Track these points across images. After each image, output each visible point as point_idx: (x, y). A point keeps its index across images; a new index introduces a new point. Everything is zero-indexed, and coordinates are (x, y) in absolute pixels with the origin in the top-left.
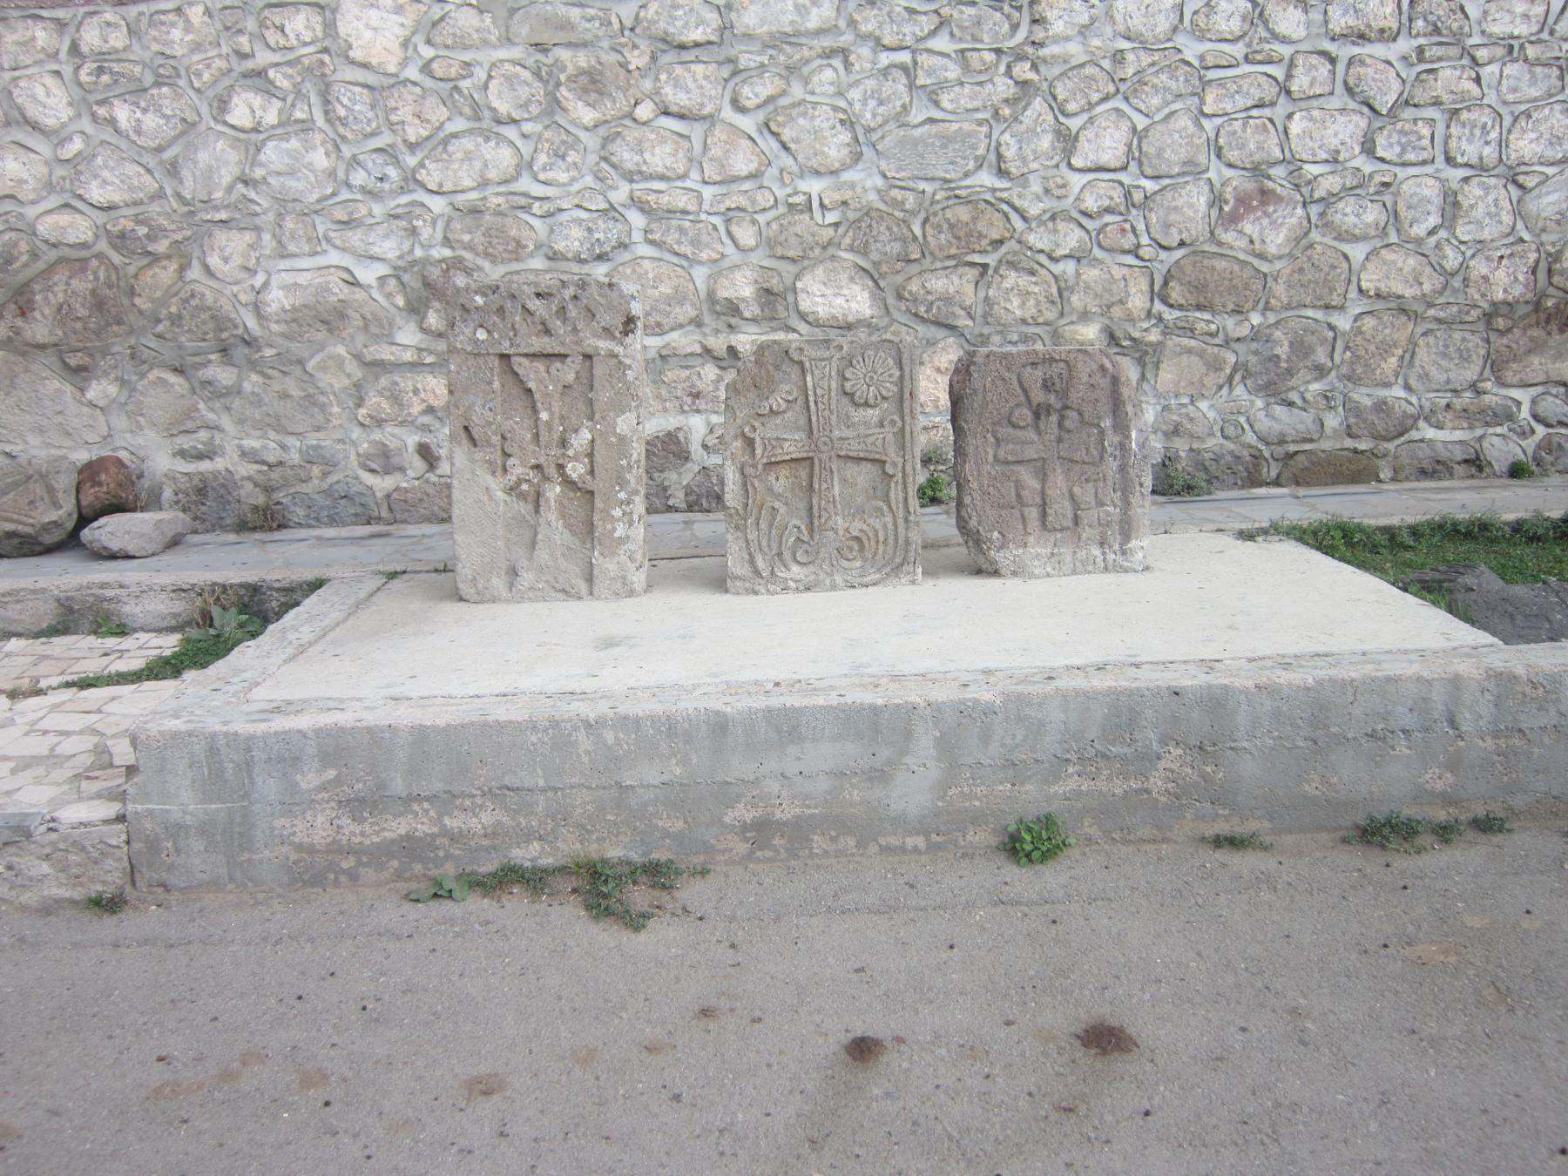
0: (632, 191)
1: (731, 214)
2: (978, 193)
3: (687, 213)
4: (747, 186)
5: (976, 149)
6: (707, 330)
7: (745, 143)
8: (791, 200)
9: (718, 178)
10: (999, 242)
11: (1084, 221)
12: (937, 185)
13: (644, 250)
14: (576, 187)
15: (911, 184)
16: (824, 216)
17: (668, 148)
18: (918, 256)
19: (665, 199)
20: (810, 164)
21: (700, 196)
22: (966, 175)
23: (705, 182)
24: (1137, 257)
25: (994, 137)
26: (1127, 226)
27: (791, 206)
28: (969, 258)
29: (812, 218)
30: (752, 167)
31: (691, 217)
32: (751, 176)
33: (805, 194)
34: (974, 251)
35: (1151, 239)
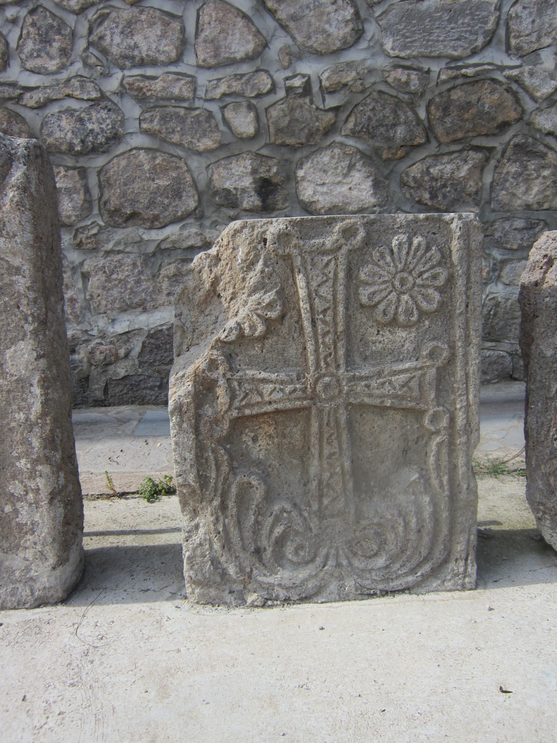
0: (123, 78)
1: (228, 100)
2: (488, 71)
3: (183, 100)
4: (245, 69)
5: (486, 23)
6: (207, 223)
7: (240, 23)
8: (289, 83)
9: (212, 62)
10: (504, 126)
12: (443, 64)
13: (138, 140)
14: (64, 75)
15: (416, 64)
16: (324, 100)
17: (158, 30)
18: (423, 141)
19: (158, 85)
20: (310, 43)
21: (193, 81)
22: (474, 52)
23: (199, 67)
25: (505, 9)
27: (289, 90)
28: (477, 142)
29: (312, 102)
30: (250, 47)
31: (186, 105)
32: (248, 59)
33: (304, 76)
34: (479, 135)
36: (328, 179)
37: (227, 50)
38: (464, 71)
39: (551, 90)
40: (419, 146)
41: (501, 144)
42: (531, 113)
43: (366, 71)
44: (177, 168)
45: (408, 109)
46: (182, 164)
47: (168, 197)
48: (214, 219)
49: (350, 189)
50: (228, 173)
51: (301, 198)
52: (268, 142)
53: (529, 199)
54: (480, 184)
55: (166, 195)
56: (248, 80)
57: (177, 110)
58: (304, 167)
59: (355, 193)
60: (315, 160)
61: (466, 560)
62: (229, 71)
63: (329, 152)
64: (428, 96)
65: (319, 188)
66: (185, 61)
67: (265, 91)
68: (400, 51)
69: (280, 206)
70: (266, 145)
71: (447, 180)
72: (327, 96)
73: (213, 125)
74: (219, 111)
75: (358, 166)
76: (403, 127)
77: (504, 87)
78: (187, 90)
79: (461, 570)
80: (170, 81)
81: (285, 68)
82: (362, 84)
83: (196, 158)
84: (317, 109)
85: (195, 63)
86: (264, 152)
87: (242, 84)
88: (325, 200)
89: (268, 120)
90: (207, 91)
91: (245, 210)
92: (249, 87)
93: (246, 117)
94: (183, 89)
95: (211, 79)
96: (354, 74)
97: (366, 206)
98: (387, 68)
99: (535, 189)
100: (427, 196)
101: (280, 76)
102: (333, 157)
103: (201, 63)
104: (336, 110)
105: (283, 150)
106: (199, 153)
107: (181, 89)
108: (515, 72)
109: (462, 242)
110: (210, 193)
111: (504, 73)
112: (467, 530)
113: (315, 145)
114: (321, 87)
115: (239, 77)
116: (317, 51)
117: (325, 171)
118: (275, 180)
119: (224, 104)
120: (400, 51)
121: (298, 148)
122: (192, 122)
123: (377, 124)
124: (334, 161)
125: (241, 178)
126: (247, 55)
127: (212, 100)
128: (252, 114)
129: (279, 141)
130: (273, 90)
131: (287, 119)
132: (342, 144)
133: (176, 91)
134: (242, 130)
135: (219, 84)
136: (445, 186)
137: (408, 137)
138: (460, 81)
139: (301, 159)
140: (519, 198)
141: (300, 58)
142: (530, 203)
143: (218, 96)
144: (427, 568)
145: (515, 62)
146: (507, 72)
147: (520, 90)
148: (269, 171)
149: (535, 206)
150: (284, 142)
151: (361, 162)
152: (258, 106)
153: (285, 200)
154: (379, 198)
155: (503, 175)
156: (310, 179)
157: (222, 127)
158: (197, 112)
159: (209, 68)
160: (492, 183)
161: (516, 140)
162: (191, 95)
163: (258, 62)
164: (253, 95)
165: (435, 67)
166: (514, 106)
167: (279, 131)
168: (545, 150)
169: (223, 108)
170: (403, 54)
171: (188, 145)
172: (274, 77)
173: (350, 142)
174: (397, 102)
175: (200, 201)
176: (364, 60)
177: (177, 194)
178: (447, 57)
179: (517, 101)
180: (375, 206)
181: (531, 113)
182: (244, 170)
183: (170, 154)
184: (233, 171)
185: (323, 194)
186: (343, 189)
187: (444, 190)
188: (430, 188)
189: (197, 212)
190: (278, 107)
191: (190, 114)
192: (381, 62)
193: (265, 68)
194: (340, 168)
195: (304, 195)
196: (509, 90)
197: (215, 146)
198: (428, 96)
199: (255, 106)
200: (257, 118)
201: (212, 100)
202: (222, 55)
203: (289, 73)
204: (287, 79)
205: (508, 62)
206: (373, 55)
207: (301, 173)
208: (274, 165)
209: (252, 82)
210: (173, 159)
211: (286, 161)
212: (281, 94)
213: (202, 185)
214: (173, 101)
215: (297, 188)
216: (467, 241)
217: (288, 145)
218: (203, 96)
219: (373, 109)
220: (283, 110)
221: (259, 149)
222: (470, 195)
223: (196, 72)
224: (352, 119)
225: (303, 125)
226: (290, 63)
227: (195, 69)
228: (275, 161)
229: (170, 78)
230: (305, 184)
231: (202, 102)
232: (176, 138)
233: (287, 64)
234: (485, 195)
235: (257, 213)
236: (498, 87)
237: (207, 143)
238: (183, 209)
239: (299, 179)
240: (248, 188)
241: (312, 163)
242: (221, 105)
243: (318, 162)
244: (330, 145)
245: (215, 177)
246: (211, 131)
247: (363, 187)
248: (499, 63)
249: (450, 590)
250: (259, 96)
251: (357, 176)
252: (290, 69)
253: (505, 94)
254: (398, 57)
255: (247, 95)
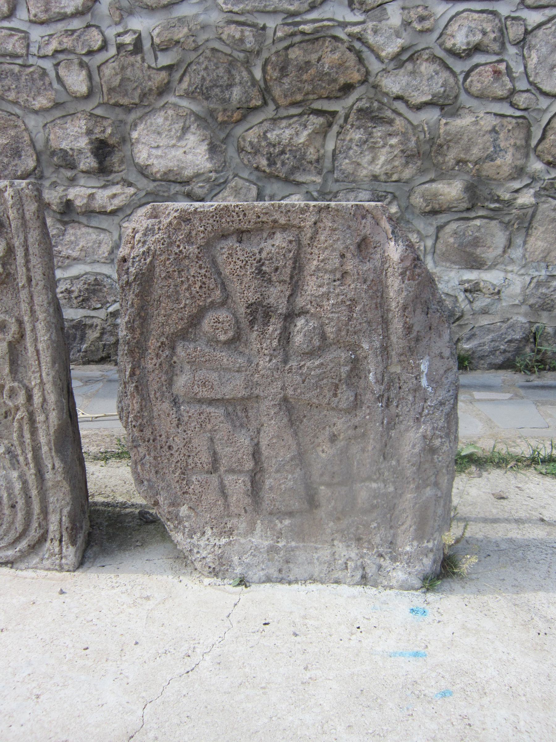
1: (61, 57)
2: (328, 27)
3: (17, 56)
4: (76, 24)
8: (120, 40)
9: (43, 17)
10: (347, 88)
11: (450, 61)
12: (279, 20)
15: (250, 19)
16: (156, 58)
18: (259, 103)
21: (26, 37)
24: (512, 105)
26: (502, 67)
27: (120, 47)
28: (317, 105)
29: (143, 60)
31: (20, 61)
32: (78, 14)
33: (135, 32)
34: (320, 98)
35: (531, 83)
36: (163, 142)
37: (58, 4)
38: (302, 27)
39: (396, 50)
40: (255, 109)
41: (343, 107)
42: (377, 74)
43: (199, 27)
44: (16, 126)
45: (242, 69)
46: (20, 123)
47: (7, 156)
48: (54, 179)
49: (185, 152)
50: (63, 134)
51: (136, 161)
52: (101, 101)
53: (376, 170)
54: (322, 151)
55: (5, 153)
56: (79, 37)
57: (12, 67)
58: (138, 129)
59: (190, 157)
60: (149, 121)
61: (61, 541)
62: (61, 26)
63: (162, 113)
64: (265, 55)
65: (154, 151)
66: (18, 17)
67: (96, 48)
68: (233, 5)
69: (116, 168)
70: (100, 105)
71: (285, 146)
72: (159, 54)
73: (47, 83)
74: (53, 68)
75: (193, 128)
76: (239, 88)
77: (346, 45)
78: (20, 47)
79: (57, 550)
80: (4, 36)
81: (117, 24)
82: (194, 41)
83: (33, 116)
84: (149, 67)
85: (27, 19)
86: (99, 112)
87: (73, 40)
88: (160, 163)
89: (101, 79)
90: (39, 48)
91: (83, 172)
92: (80, 44)
93: (78, 75)
94: (17, 45)
95: (43, 35)
96: (186, 30)
97: (202, 171)
98: (221, 24)
99: (382, 159)
100: (264, 162)
101: (111, 32)
102: (166, 119)
103: (32, 18)
104: (170, 68)
105: (118, 110)
106: (36, 112)
107: (14, 45)
108: (356, 29)
109: (15, 211)
110: (48, 153)
111: (346, 30)
112: (59, 510)
113: (149, 106)
114: (152, 44)
115: (70, 33)
116: (148, 5)
117: (159, 133)
118: (111, 142)
119: (58, 61)
120: (233, 5)
121: (133, 108)
122: (26, 79)
123: (211, 84)
124: (168, 123)
125: (76, 138)
126: (77, 9)
127: (45, 57)
128: (84, 72)
129: (112, 101)
130: (104, 47)
131: (119, 78)
132: (175, 105)
133: (10, 47)
134: (76, 89)
135: (51, 40)
136: (283, 152)
137: (243, 99)
138: (298, 39)
139: (134, 120)
140: (364, 168)
141: (131, 13)
142: (377, 174)
143: (50, 53)
144: (23, 544)
145: (359, 17)
146: (349, 29)
147: (364, 49)
148: (104, 132)
149: (383, 178)
150: (117, 102)
151: (196, 125)
152: (89, 64)
153: (122, 162)
154: (215, 163)
155: (346, 143)
156: (144, 141)
157: (56, 85)
158: (31, 69)
159: (42, 23)
160: (334, 150)
161: (359, 104)
162: (24, 51)
163: (88, 17)
164: (84, 52)
165: (271, 23)
166: (357, 67)
167: (111, 90)
168: (393, 116)
169: (57, 65)
170: (236, 9)
171: (25, 103)
172: (106, 34)
173: (184, 103)
174: (231, 61)
175: (38, 160)
176: (197, 15)
177: (17, 153)
178: (282, 12)
179: (361, 60)
180: (211, 172)
181: (377, 74)
182: (79, 130)
183: (8, 112)
184: (69, 130)
185: (157, 157)
186: (178, 153)
187: (282, 157)
188: (267, 154)
189: (36, 172)
190: (110, 65)
191: (25, 71)
192: (215, 17)
193: (97, 24)
194: (173, 130)
195: (139, 158)
196: (351, 49)
197: (50, 105)
198: (265, 55)
199: (87, 64)
200: (90, 77)
201: (45, 57)
202: (53, 9)
203: (120, 29)
204: (119, 35)
205: (351, 17)
206: (206, 10)
207: (135, 135)
208: (109, 126)
209: (83, 38)
210: (13, 117)
211: (121, 121)
212: (113, 51)
213: (40, 145)
214: (8, 58)
215: (132, 151)
216: (21, 211)
217: (122, 105)
218: (36, 53)
219: (206, 69)
220: (114, 68)
221: (93, 109)
222: (311, 163)
223: (29, 28)
224: (186, 79)
225: (136, 84)
226: (122, 18)
227: (28, 24)
228: (110, 121)
229: (3, 34)
230: (140, 146)
231: (35, 58)
232: (12, 96)
233: (118, 19)
234: (327, 163)
235: (94, 175)
236: (340, 45)
237: (41, 102)
238: (23, 169)
239: (133, 141)
240: (84, 149)
241: (146, 124)
242: (55, 62)
243: (152, 124)
244: (164, 106)
245: (52, 137)
246: (45, 89)
247: (198, 151)
248: (341, 19)
249: (49, 569)
250: (90, 53)
251: (192, 139)
252: (122, 25)
253: (348, 52)
254: (231, 12)
255: (78, 52)
